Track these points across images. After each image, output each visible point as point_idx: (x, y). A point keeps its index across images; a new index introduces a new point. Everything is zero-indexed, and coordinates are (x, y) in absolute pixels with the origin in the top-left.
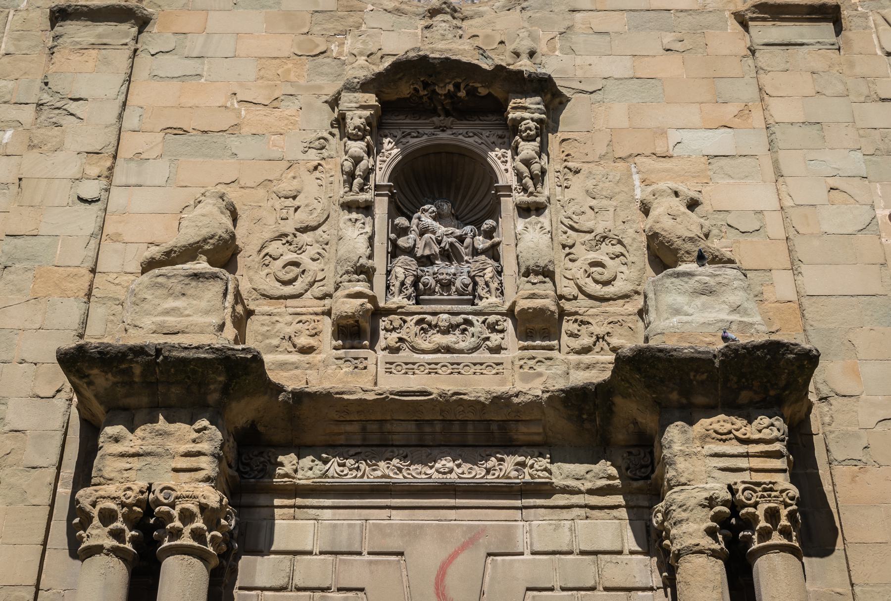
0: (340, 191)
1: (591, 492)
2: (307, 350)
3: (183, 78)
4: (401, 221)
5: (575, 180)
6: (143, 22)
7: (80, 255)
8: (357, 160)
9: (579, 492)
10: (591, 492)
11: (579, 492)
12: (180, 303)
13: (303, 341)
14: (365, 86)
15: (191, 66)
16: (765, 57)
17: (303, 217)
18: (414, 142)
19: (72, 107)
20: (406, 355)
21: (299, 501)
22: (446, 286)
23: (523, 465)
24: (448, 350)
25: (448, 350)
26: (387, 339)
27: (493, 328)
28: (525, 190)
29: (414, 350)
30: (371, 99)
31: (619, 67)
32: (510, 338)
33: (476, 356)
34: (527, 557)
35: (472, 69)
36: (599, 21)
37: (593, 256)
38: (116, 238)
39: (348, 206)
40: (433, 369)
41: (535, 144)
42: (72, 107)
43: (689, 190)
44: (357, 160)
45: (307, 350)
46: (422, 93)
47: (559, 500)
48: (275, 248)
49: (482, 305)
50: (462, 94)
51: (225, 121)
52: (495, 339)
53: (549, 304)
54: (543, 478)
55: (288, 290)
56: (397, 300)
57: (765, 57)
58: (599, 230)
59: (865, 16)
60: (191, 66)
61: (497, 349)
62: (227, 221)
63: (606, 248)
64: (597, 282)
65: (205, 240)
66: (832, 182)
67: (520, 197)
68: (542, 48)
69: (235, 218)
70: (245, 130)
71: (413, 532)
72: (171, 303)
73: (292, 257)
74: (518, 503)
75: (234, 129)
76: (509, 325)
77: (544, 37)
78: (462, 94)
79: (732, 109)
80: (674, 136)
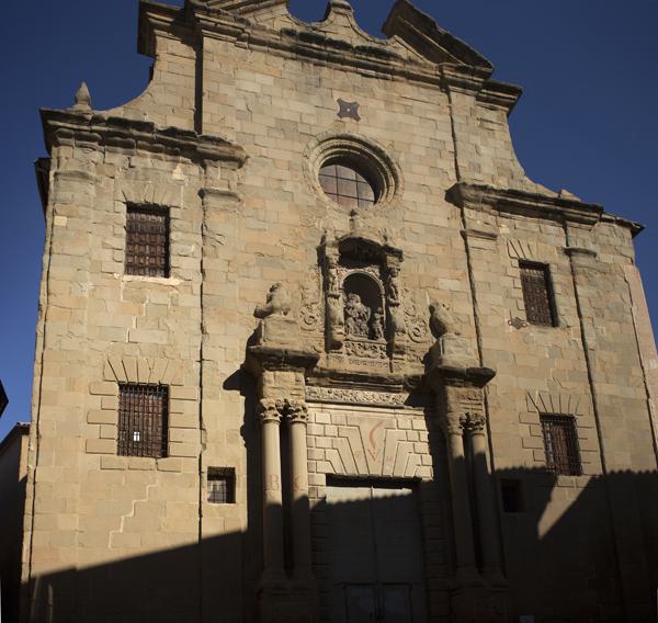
3: (260, 230)
12: (285, 332)
14: (334, 245)
15: (260, 225)
18: (351, 271)
19: (218, 238)
29: (357, 355)
31: (420, 248)
40: (365, 363)
42: (218, 238)
46: (356, 251)
55: (310, 327)
56: (350, 336)
60: (260, 225)
70: (286, 258)
71: (360, 420)
72: (280, 332)
75: (283, 256)
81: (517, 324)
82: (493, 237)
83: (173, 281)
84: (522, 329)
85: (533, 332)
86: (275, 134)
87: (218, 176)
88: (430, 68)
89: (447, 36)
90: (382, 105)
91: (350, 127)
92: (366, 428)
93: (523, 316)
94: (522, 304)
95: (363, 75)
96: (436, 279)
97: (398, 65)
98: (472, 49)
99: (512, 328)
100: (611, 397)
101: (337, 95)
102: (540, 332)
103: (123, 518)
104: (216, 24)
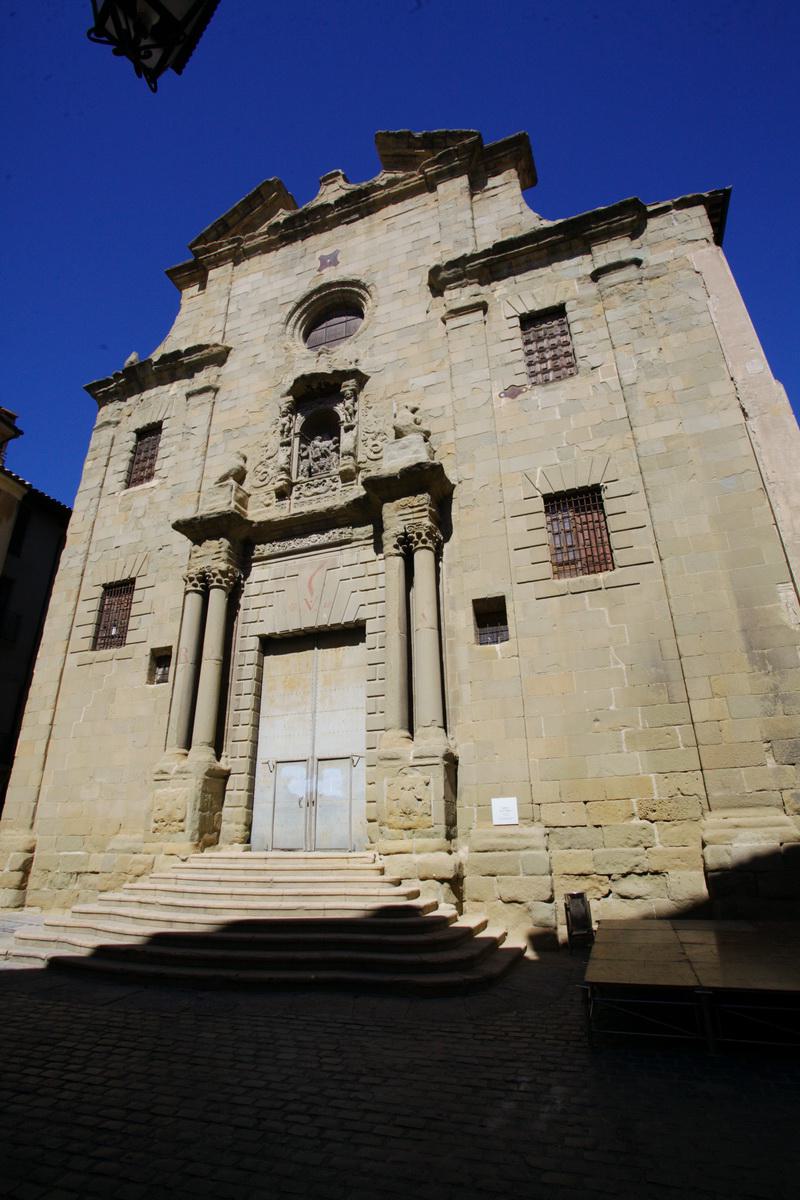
0: (280, 440)
1: (366, 539)
2: (268, 505)
3: (230, 409)
4: (303, 446)
5: (370, 412)
6: (216, 390)
7: (194, 487)
8: (284, 425)
9: (361, 540)
10: (366, 539)
11: (361, 540)
13: (267, 502)
16: (454, 335)
17: (269, 454)
18: (310, 412)
19: (193, 431)
20: (303, 499)
21: (265, 562)
22: (322, 468)
23: (342, 533)
24: (318, 494)
25: (318, 494)
26: (295, 494)
27: (333, 481)
28: (348, 421)
29: (305, 496)
30: (291, 398)
31: (390, 357)
32: (339, 485)
33: (325, 495)
34: (342, 568)
35: (323, 375)
36: (384, 339)
37: (374, 443)
38: (207, 478)
39: (282, 445)
41: (351, 401)
42: (193, 431)
43: (413, 405)
44: (284, 425)
45: (268, 505)
47: (354, 544)
48: (260, 468)
49: (331, 472)
50: (323, 387)
51: (246, 420)
52: (334, 485)
53: (351, 467)
54: (348, 537)
55: (264, 483)
56: (301, 478)
57: (451, 333)
58: (377, 431)
59: (499, 303)
61: (334, 490)
62: (241, 463)
63: (380, 437)
64: (375, 453)
65: (230, 471)
66: (474, 386)
67: (346, 424)
68: (361, 358)
69: (245, 459)
72: (214, 498)
73: (264, 470)
74: (339, 548)
75: (246, 425)
76: (339, 478)
77: (362, 351)
78: (323, 387)
79: (437, 363)
80: (411, 382)
81: (513, 392)
82: (483, 307)
83: (154, 482)
84: (520, 397)
85: (538, 396)
86: (258, 317)
87: (201, 379)
88: (416, 178)
89: (425, 135)
90: (363, 238)
91: (331, 275)
92: (305, 574)
93: (523, 380)
94: (522, 367)
95: (348, 223)
96: (406, 381)
97: (378, 195)
98: (451, 131)
99: (504, 401)
100: (667, 439)
101: (318, 255)
102: (547, 391)
103: (84, 709)
104: (215, 255)
